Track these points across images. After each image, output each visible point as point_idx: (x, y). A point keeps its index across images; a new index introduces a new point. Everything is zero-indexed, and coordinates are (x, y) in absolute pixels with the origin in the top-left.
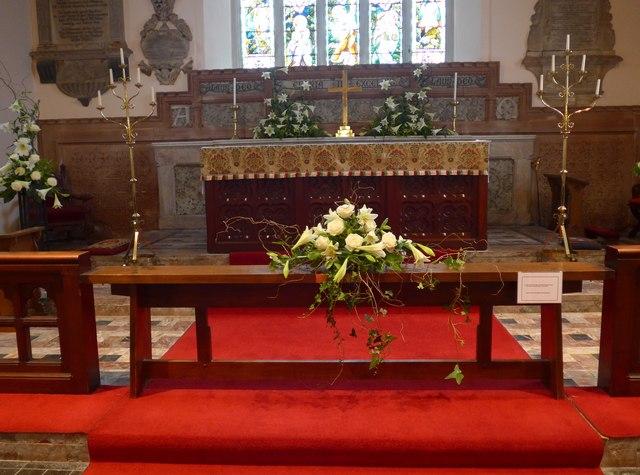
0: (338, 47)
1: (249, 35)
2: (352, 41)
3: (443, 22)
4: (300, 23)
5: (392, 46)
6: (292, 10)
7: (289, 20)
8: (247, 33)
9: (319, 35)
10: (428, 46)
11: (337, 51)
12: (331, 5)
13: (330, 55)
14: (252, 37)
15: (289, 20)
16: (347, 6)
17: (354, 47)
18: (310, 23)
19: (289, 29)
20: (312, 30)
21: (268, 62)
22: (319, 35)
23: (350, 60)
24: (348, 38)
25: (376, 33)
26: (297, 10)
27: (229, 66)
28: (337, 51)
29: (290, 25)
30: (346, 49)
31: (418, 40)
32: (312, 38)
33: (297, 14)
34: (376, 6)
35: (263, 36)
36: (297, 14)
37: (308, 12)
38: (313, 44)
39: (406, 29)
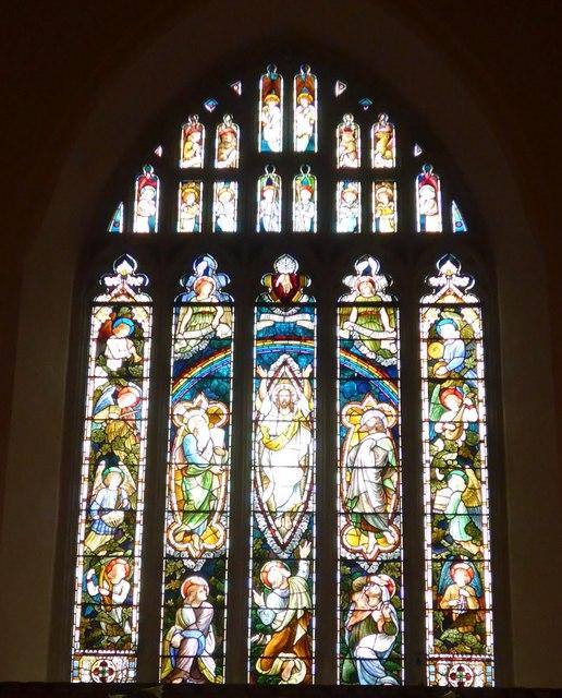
0: (271, 642)
1: (89, 610)
2: (300, 632)
3: (488, 599)
4: (199, 587)
5: (384, 644)
6: (179, 565)
7: (173, 585)
8: (84, 606)
9: (234, 619)
10: (461, 648)
11: (267, 651)
12: (264, 556)
13: (254, 659)
14: (94, 614)
15: (173, 585)
16: (292, 564)
17: (305, 641)
18: (214, 592)
19: (171, 602)
20: (218, 607)
21: (121, 668)
22: (234, 619)
23: (295, 672)
24: (292, 625)
25: (351, 621)
26: (189, 563)
27: (41, 676)
28: (267, 651)
29: (174, 594)
30: (288, 648)
31: (437, 634)
32: (216, 621)
33: (190, 572)
34: (353, 564)
35: (118, 614)
36: (190, 572)
37: (212, 569)
38: (218, 634)
39: (412, 609)
